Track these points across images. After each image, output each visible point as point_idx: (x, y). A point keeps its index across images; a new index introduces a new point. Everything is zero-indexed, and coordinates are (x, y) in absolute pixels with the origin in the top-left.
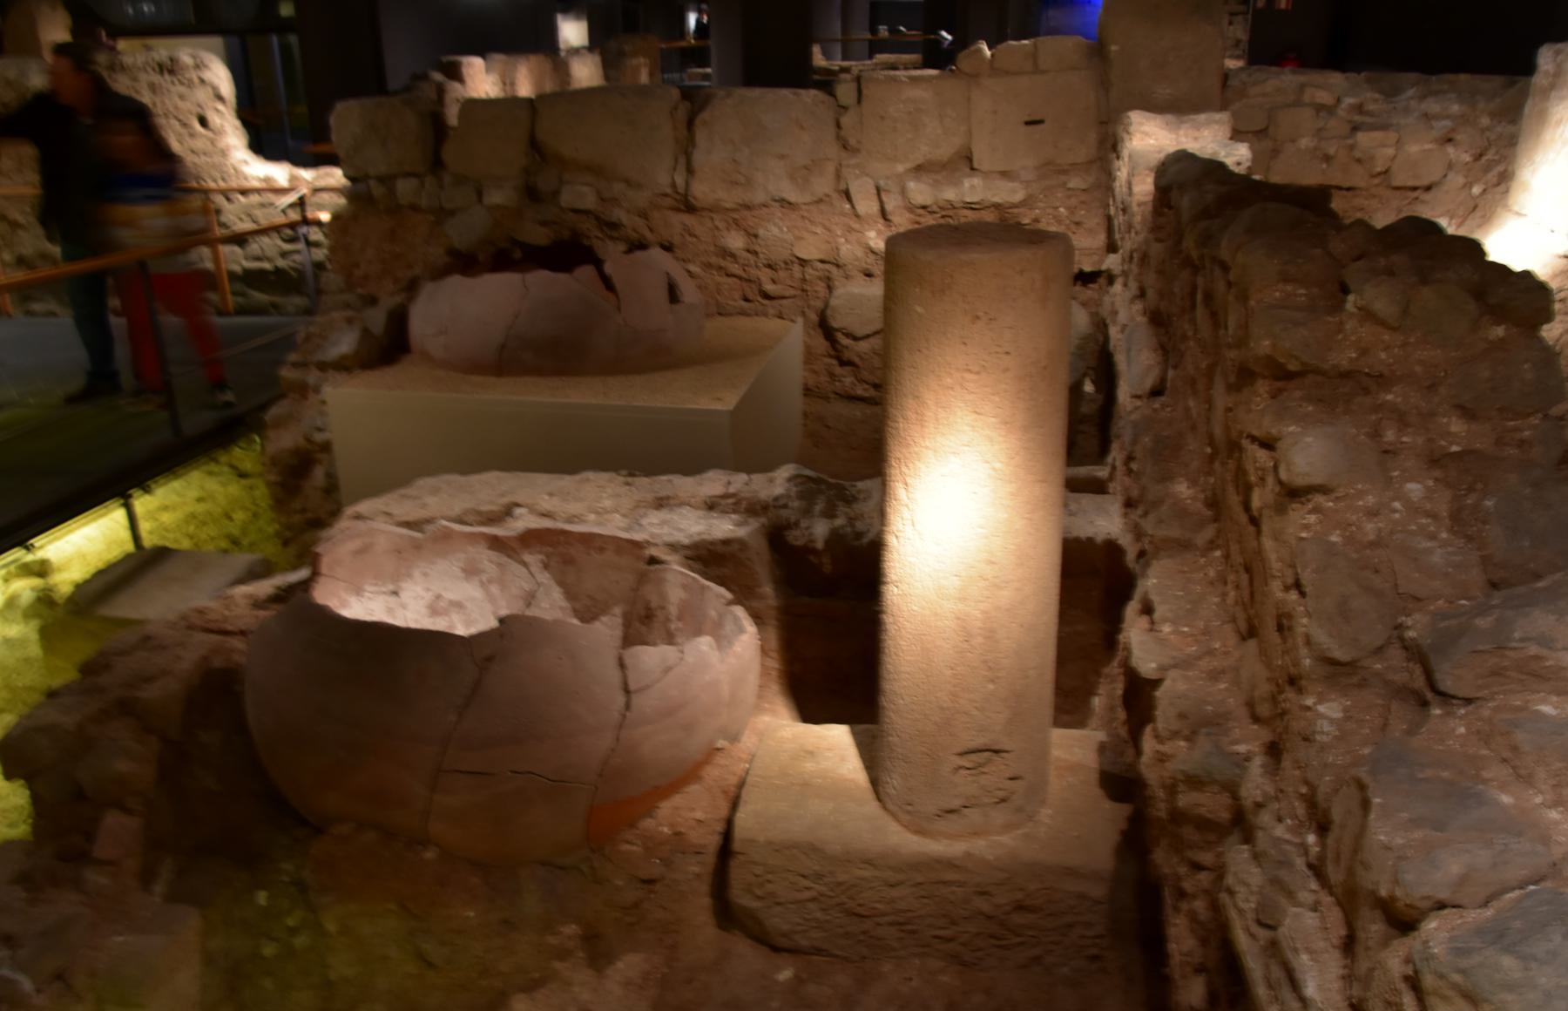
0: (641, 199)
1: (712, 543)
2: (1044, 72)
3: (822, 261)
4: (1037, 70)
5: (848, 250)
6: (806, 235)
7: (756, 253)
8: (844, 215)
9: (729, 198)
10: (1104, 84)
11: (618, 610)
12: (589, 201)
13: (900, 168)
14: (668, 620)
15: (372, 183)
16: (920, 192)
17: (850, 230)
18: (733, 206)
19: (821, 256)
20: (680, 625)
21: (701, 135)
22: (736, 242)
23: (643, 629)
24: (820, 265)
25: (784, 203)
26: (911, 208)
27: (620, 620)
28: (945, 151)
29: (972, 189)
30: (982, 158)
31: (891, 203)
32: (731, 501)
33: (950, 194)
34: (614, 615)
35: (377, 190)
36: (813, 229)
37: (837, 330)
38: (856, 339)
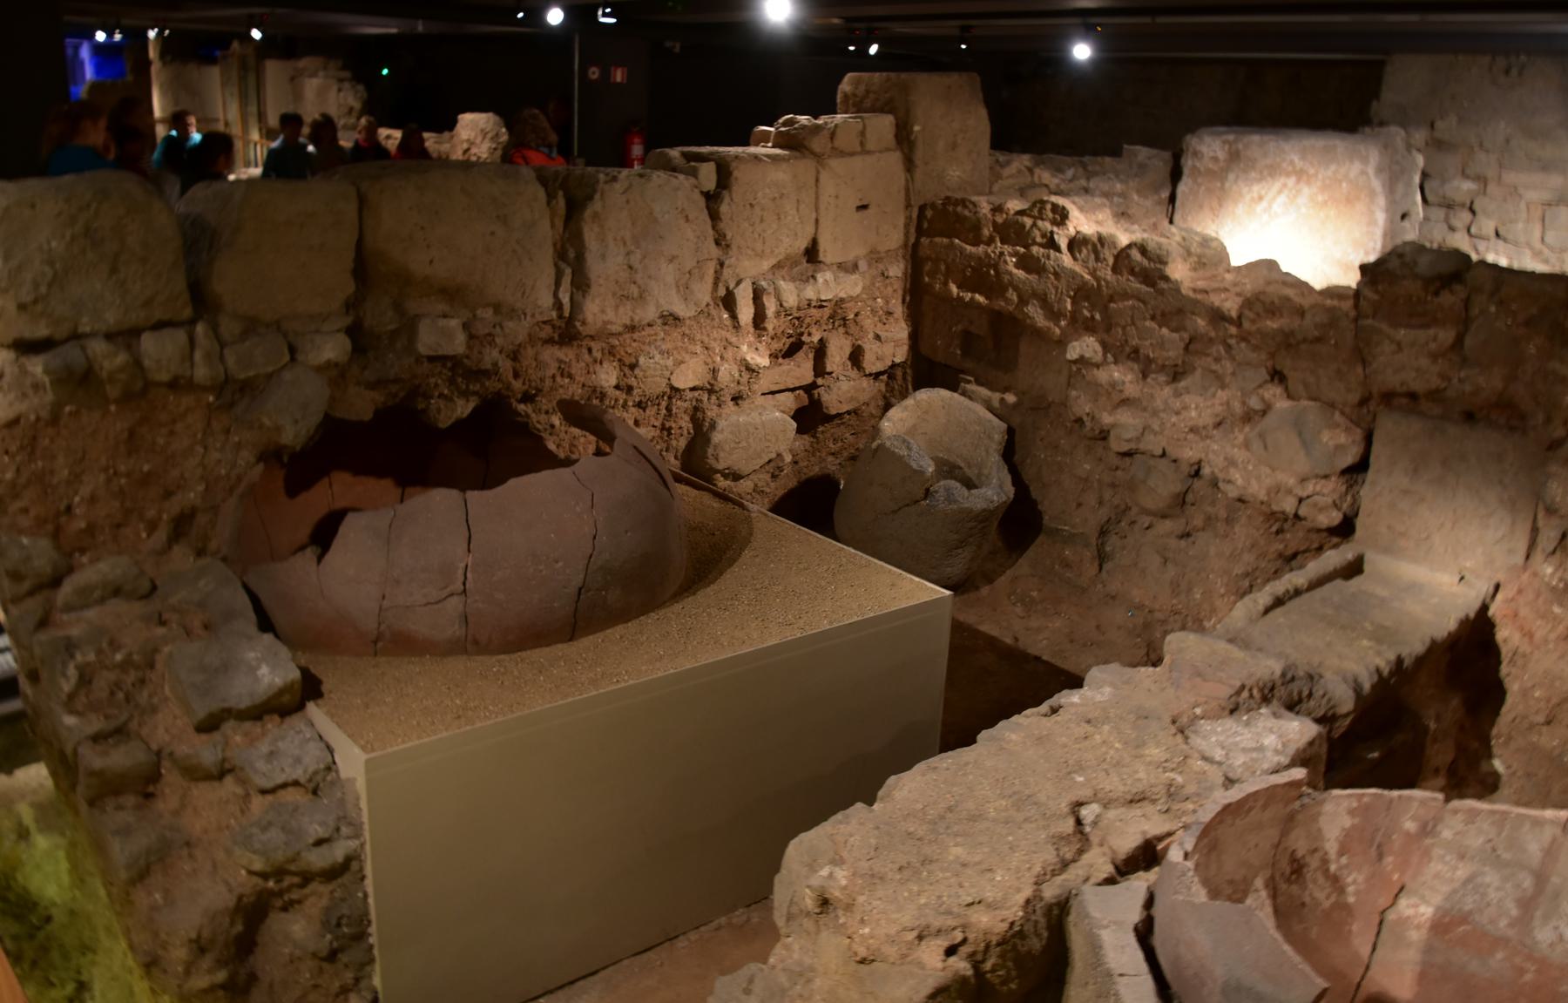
0: (518, 330)
1: (1304, 750)
2: (869, 152)
3: (693, 389)
4: (865, 152)
5: (728, 373)
6: (687, 357)
7: (630, 389)
8: (721, 326)
9: (617, 318)
10: (909, 164)
11: (1259, 883)
12: (457, 344)
13: (766, 265)
14: (1325, 861)
15: (98, 347)
16: (791, 294)
17: (727, 344)
18: (620, 329)
19: (691, 385)
20: (1344, 860)
21: (590, 235)
22: (608, 376)
23: (1295, 889)
24: (689, 395)
25: (670, 319)
26: (782, 310)
27: (1264, 894)
28: (802, 244)
29: (827, 286)
30: (828, 252)
31: (771, 306)
32: (1245, 694)
33: (810, 293)
34: (1257, 890)
35: (109, 359)
36: (692, 348)
37: (718, 471)
38: (736, 477)
